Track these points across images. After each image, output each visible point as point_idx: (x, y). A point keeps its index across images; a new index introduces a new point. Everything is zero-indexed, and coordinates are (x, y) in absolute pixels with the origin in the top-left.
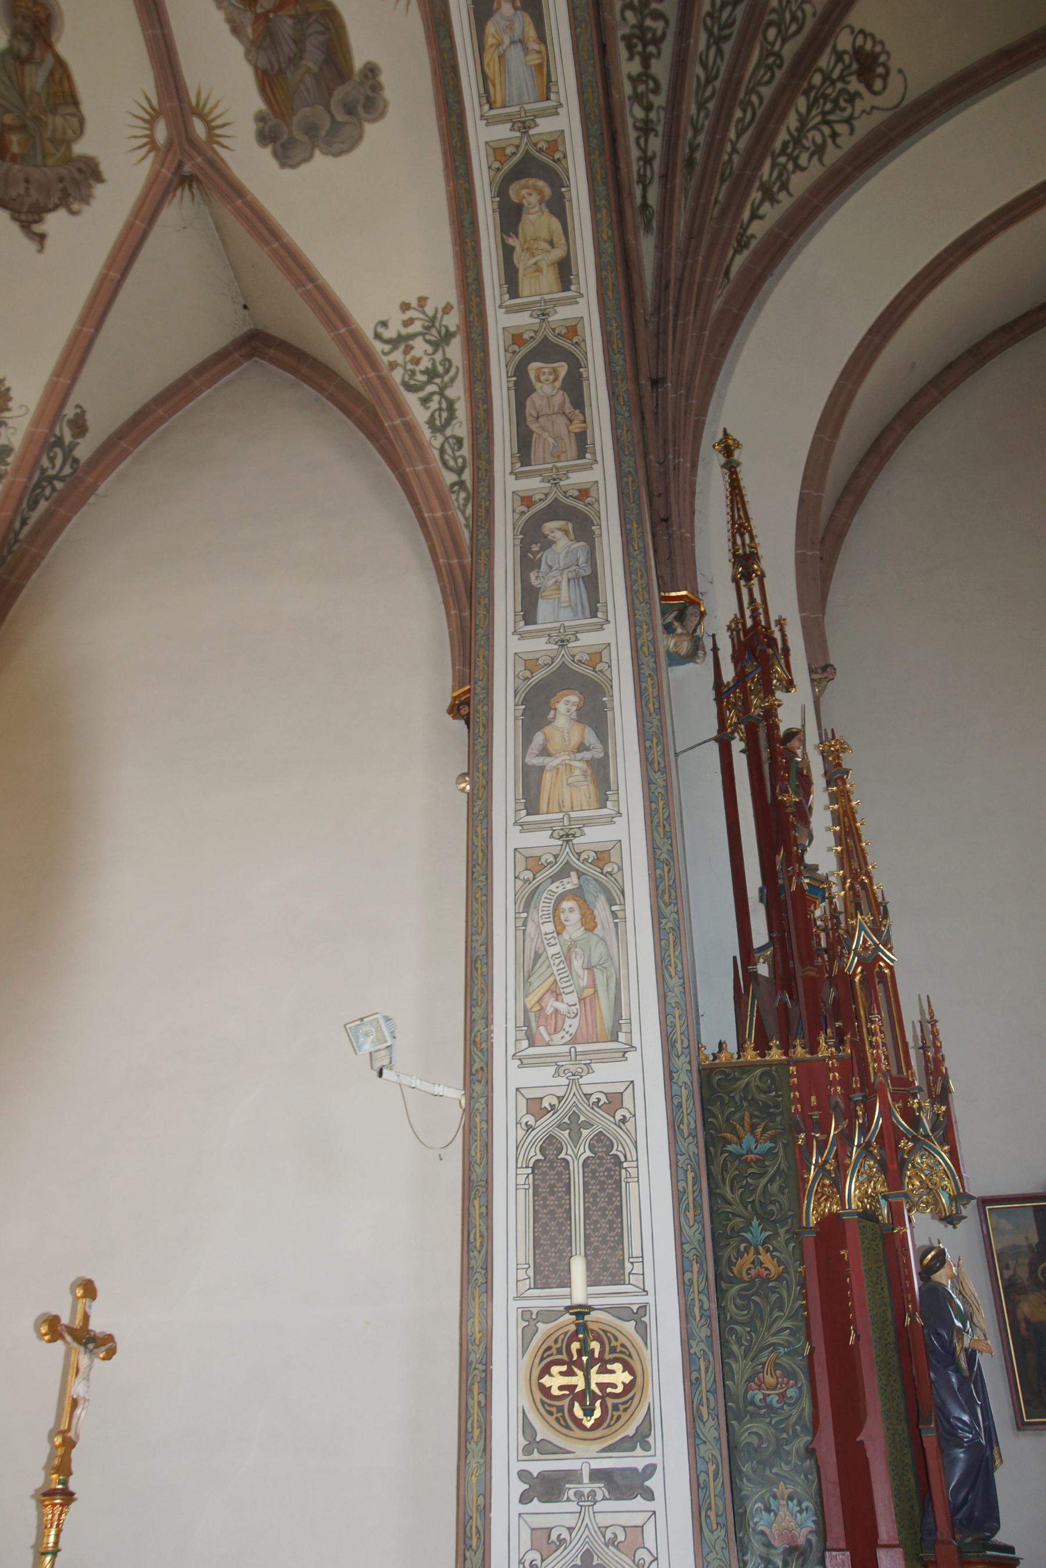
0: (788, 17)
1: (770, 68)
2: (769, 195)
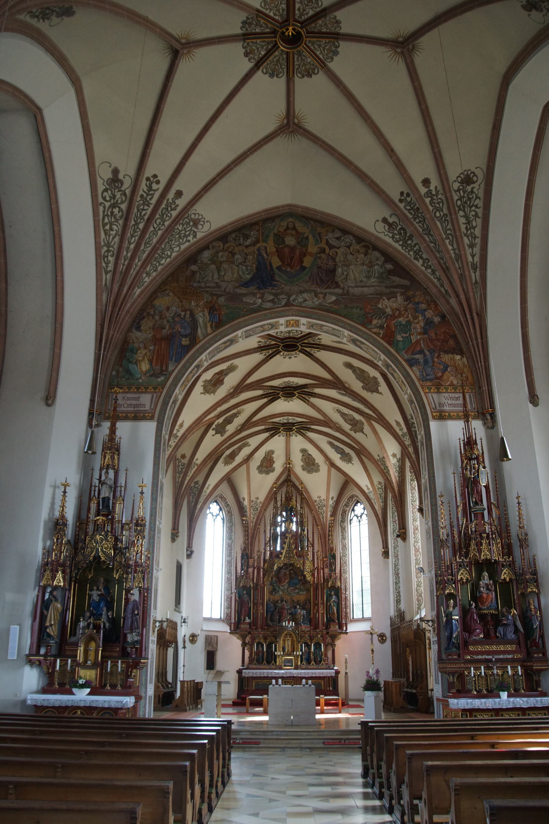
0: (437, 205)
1: (445, 220)
2: (472, 246)
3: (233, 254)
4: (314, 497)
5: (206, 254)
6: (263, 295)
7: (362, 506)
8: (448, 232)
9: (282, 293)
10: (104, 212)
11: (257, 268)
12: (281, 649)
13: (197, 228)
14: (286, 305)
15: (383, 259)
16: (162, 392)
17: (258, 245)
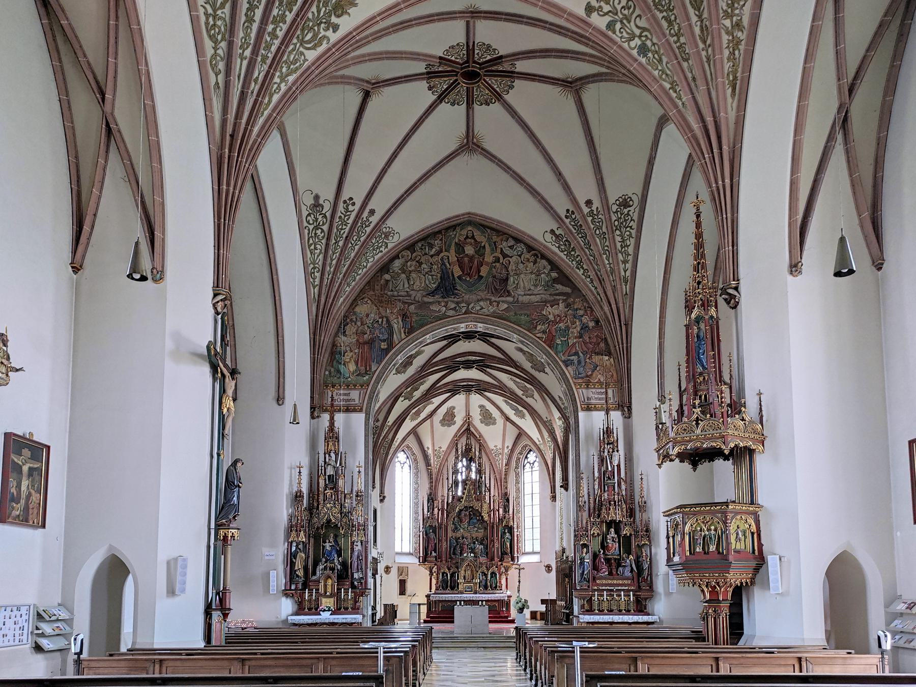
2: (625, 262)
3: (421, 264)
4: (491, 446)
5: (397, 263)
6: (447, 303)
7: (535, 454)
8: (606, 248)
9: (463, 302)
10: (309, 234)
11: (441, 278)
12: (463, 578)
13: (388, 240)
14: (465, 313)
15: (549, 267)
17: (442, 255)
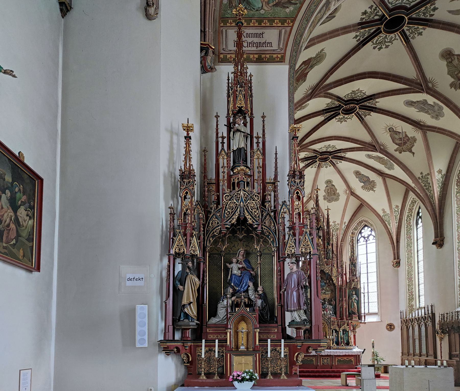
7: (370, 229)
16: (292, 27)
